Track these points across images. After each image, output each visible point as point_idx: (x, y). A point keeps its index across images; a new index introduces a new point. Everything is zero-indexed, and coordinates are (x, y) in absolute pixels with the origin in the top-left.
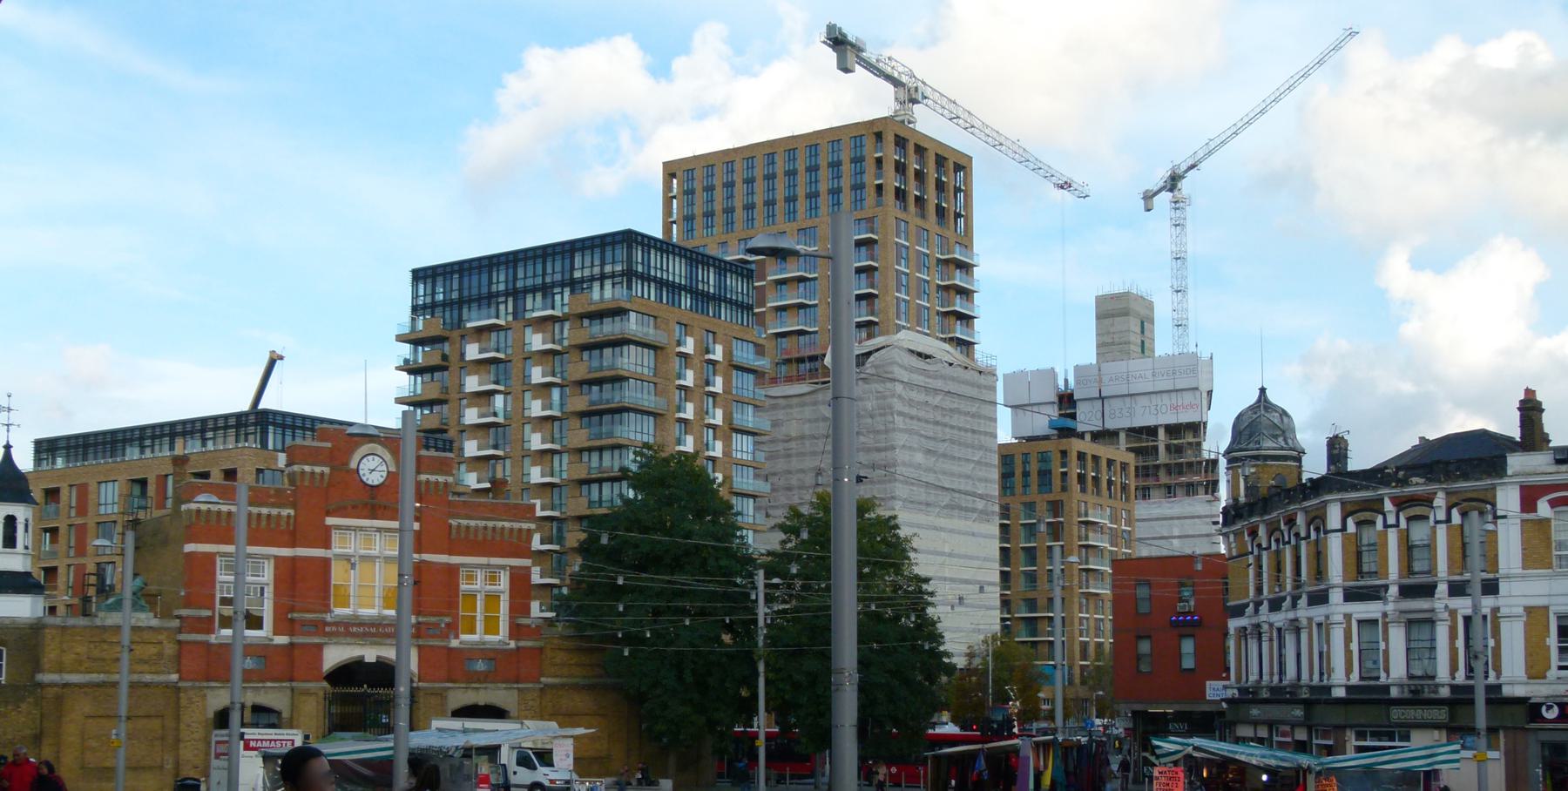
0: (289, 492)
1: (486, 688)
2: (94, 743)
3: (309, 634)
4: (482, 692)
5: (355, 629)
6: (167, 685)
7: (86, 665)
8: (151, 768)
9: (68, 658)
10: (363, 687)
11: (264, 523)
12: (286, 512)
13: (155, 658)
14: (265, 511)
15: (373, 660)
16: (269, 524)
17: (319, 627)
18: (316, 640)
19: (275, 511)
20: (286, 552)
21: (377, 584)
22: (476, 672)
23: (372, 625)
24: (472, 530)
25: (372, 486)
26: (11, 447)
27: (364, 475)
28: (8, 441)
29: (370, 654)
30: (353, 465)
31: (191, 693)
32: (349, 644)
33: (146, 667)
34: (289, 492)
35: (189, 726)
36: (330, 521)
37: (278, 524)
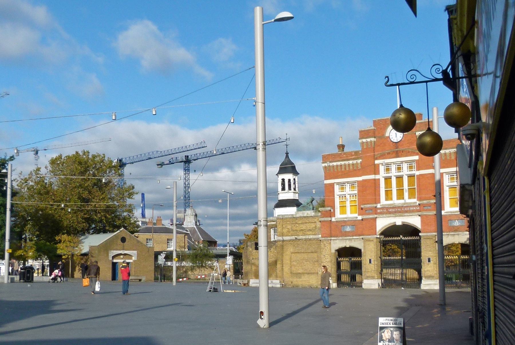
0: (360, 152)
1: (458, 235)
2: (295, 263)
3: (369, 214)
4: (456, 236)
5: (391, 210)
6: (317, 239)
7: (291, 233)
8: (314, 273)
9: (285, 231)
10: (400, 237)
11: (351, 167)
12: (359, 161)
13: (314, 228)
14: (351, 162)
15: (400, 224)
16: (353, 168)
17: (375, 210)
18: (371, 216)
19: (355, 162)
20: (360, 179)
21: (416, 187)
22: (454, 227)
23: (399, 207)
24: (448, 155)
25: (396, 143)
26: (288, 153)
27: (392, 138)
28: (287, 151)
29: (399, 221)
30: (387, 135)
31: (325, 242)
32: (388, 217)
33: (311, 232)
34: (360, 152)
35: (325, 256)
36: (377, 162)
37: (357, 167)
